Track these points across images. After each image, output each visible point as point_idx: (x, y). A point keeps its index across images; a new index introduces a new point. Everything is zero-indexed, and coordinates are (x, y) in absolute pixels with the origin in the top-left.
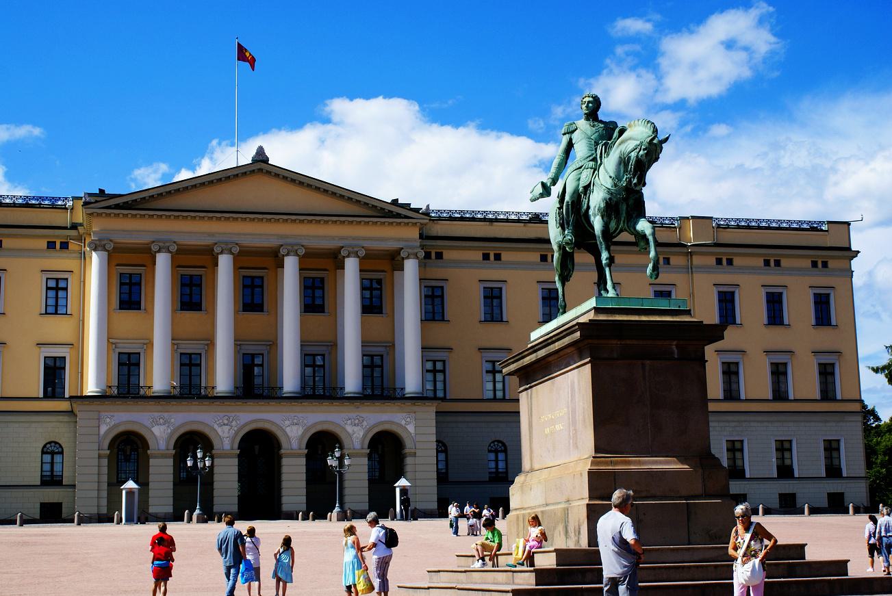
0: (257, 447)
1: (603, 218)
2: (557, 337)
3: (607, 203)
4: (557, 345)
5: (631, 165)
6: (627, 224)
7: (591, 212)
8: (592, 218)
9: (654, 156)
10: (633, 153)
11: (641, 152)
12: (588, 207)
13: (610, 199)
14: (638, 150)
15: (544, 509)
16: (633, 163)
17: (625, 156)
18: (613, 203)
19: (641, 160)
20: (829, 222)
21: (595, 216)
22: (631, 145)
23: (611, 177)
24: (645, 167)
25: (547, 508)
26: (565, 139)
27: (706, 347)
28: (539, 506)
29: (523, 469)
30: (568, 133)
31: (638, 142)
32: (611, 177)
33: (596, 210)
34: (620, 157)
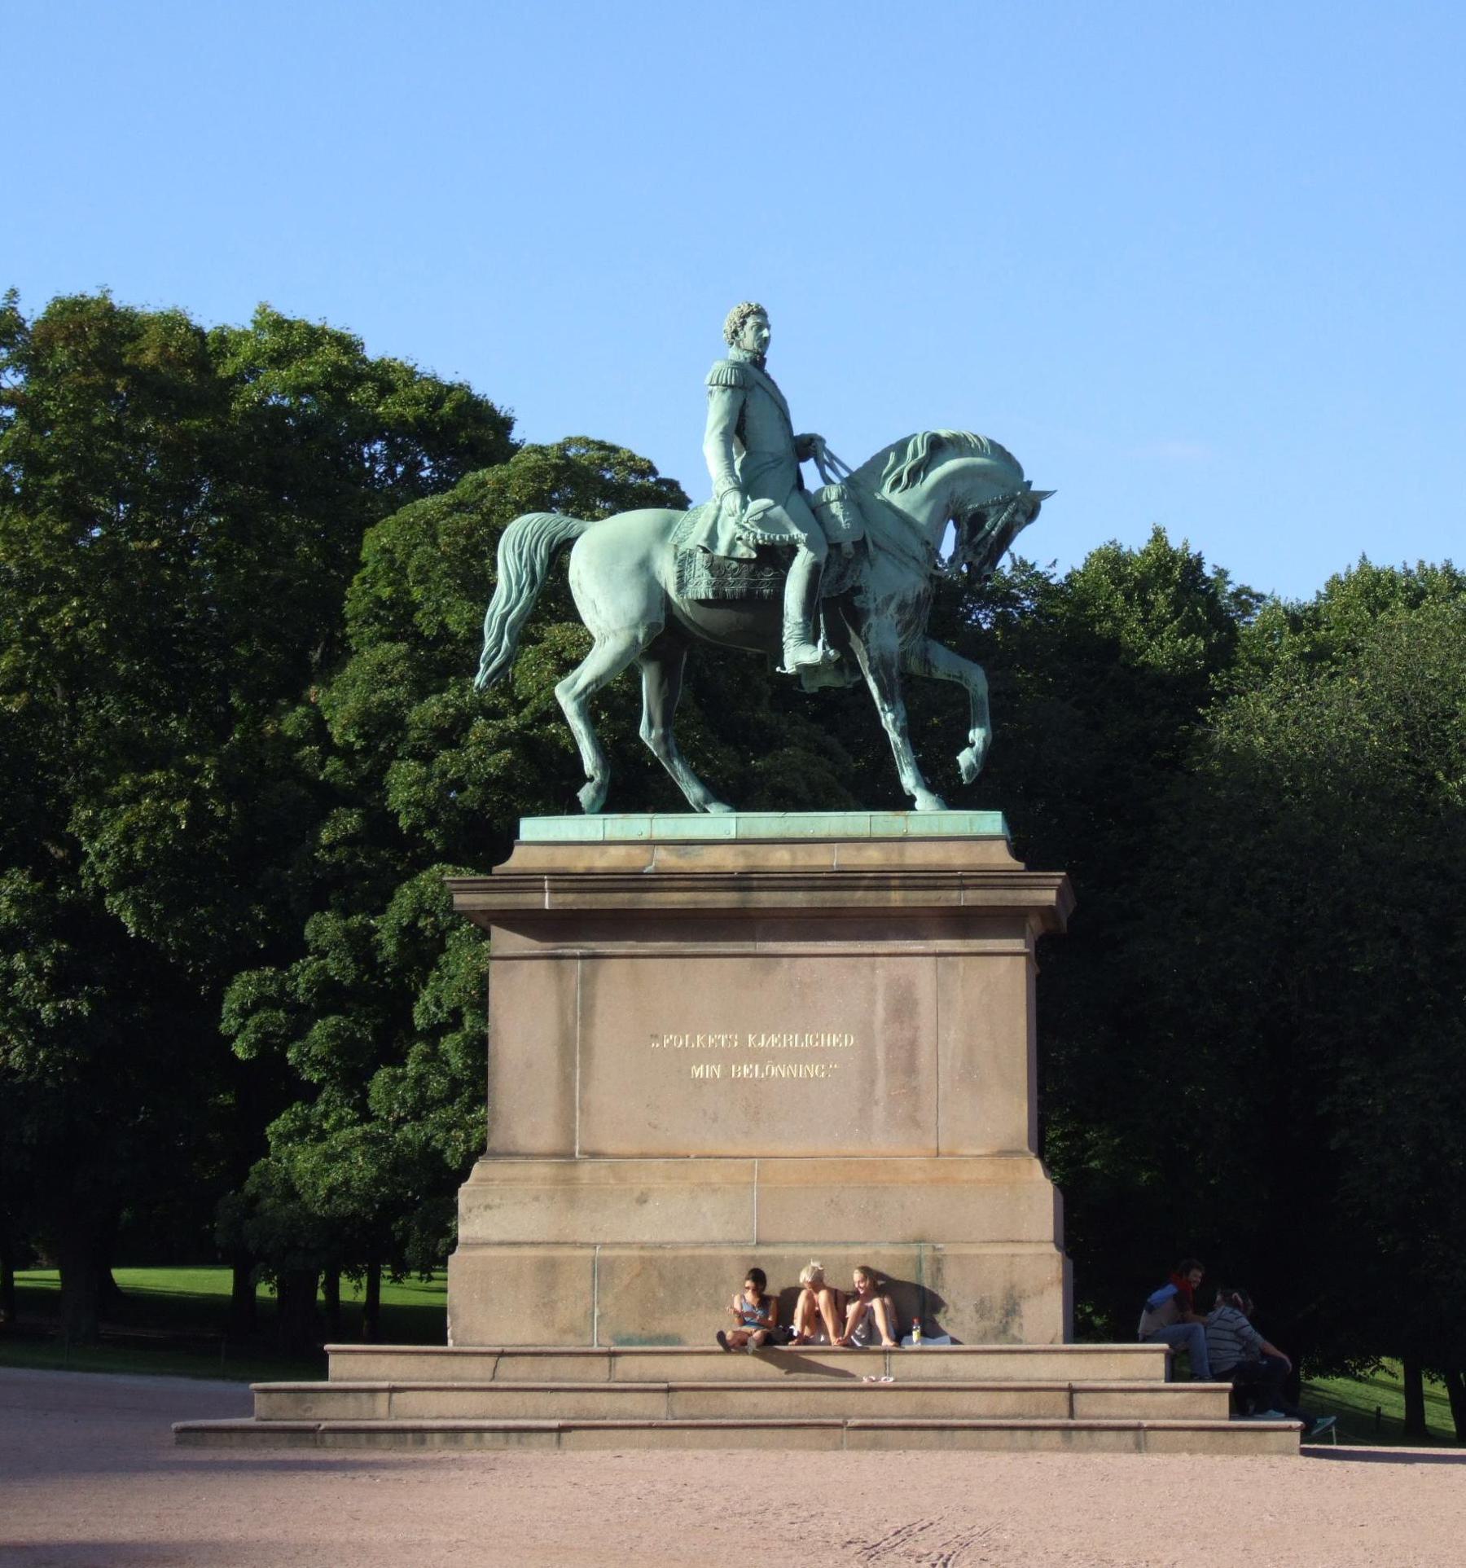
12: (857, 590)
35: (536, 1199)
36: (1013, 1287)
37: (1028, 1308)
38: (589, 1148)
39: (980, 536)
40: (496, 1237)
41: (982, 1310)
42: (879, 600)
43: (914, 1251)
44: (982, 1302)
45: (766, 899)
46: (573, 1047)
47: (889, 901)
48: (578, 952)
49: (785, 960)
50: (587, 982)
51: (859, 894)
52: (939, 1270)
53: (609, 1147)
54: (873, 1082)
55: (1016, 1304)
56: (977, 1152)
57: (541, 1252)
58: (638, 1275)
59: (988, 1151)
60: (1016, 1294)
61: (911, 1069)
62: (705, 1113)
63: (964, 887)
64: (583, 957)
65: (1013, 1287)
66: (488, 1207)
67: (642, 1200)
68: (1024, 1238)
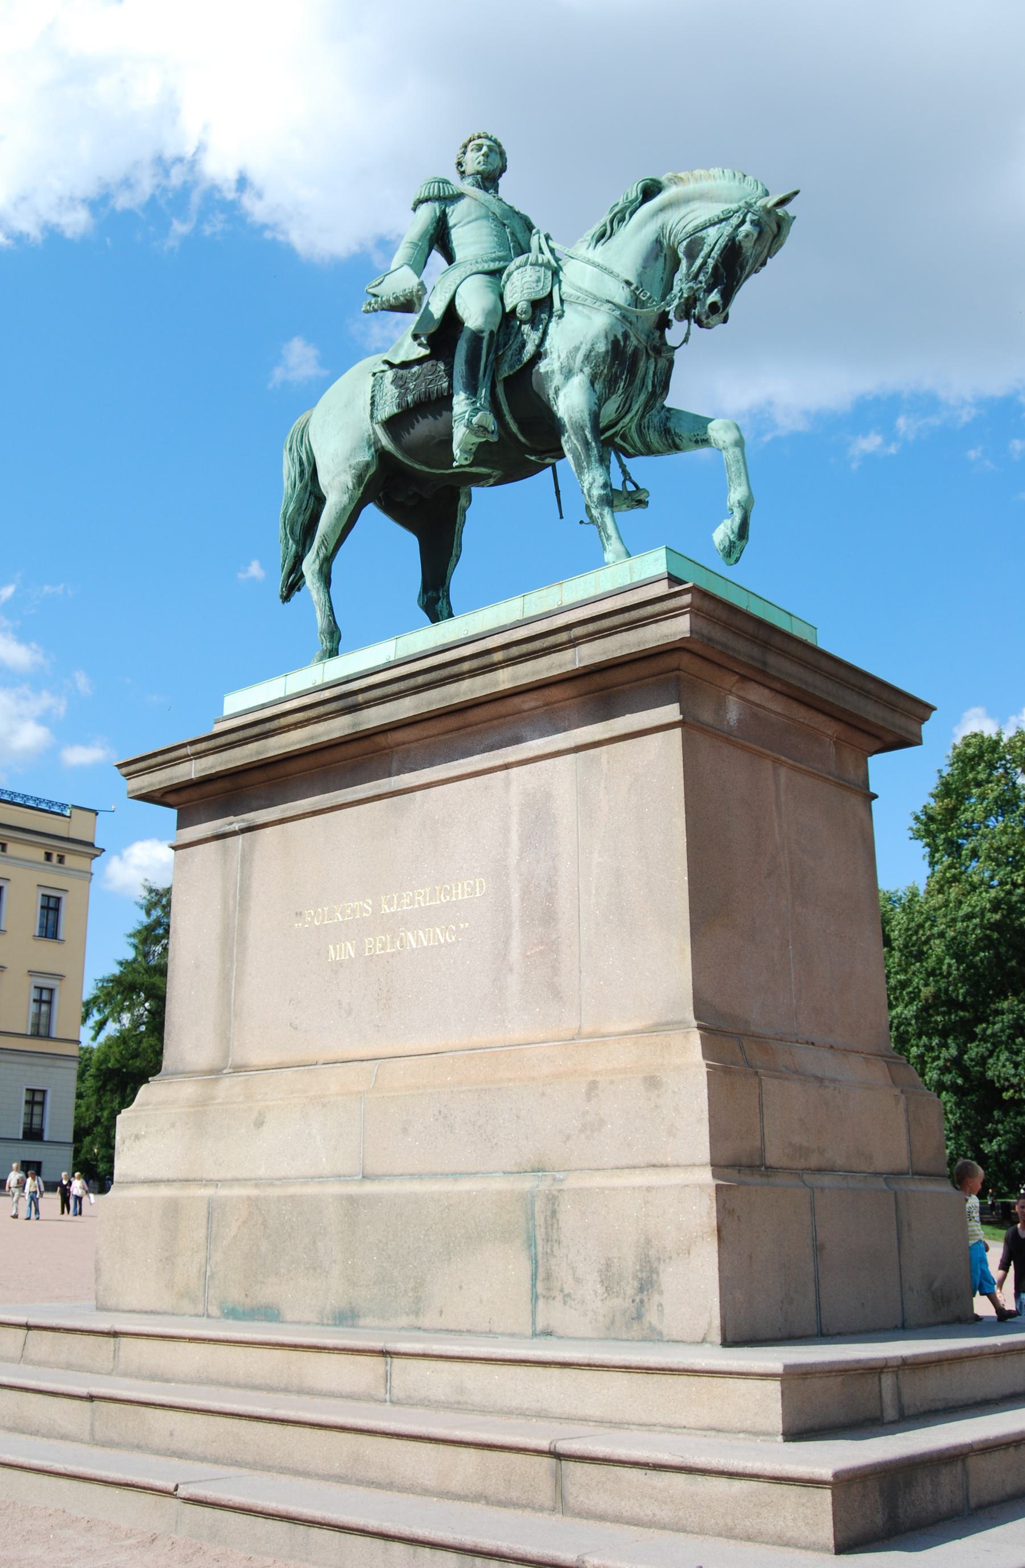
0: (108, 240)
1: (592, 383)
2: (591, 628)
3: (615, 343)
4: (504, 679)
5: (709, 255)
6: (642, 417)
7: (543, 367)
8: (557, 380)
9: (766, 251)
10: (712, 233)
11: (747, 227)
12: (538, 355)
13: (626, 336)
14: (735, 221)
15: (353, 1189)
16: (715, 254)
17: (680, 236)
18: (630, 350)
19: (740, 247)
20: (74, 807)
21: (568, 374)
22: (702, 212)
23: (628, 283)
24: (743, 268)
25: (370, 1188)
26: (427, 212)
27: (869, 759)
28: (340, 1178)
29: (167, 1062)
30: (439, 199)
31: (734, 206)
32: (628, 283)
33: (580, 357)
34: (658, 242)
35: (173, 1125)
36: (648, 1241)
37: (669, 1277)
38: (239, 1061)
39: (699, 262)
40: (142, 1175)
41: (609, 1280)
42: (563, 356)
43: (527, 1184)
44: (608, 1266)
45: (374, 717)
46: (232, 940)
47: (497, 684)
48: (236, 827)
49: (419, 793)
50: (246, 859)
51: (466, 684)
52: (554, 1213)
53: (255, 1058)
54: (506, 943)
55: (653, 1271)
56: (626, 1027)
57: (164, 1192)
58: (244, 1222)
59: (637, 1025)
60: (652, 1253)
61: (549, 917)
62: (340, 1003)
63: (573, 643)
64: (243, 831)
65: (648, 1241)
66: (137, 1137)
67: (259, 1123)
68: (669, 1160)
